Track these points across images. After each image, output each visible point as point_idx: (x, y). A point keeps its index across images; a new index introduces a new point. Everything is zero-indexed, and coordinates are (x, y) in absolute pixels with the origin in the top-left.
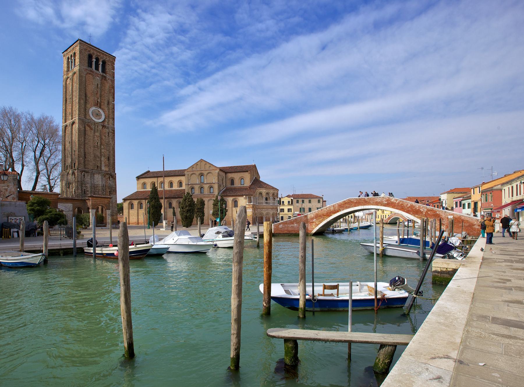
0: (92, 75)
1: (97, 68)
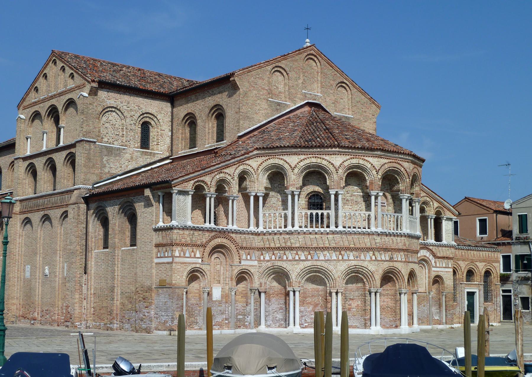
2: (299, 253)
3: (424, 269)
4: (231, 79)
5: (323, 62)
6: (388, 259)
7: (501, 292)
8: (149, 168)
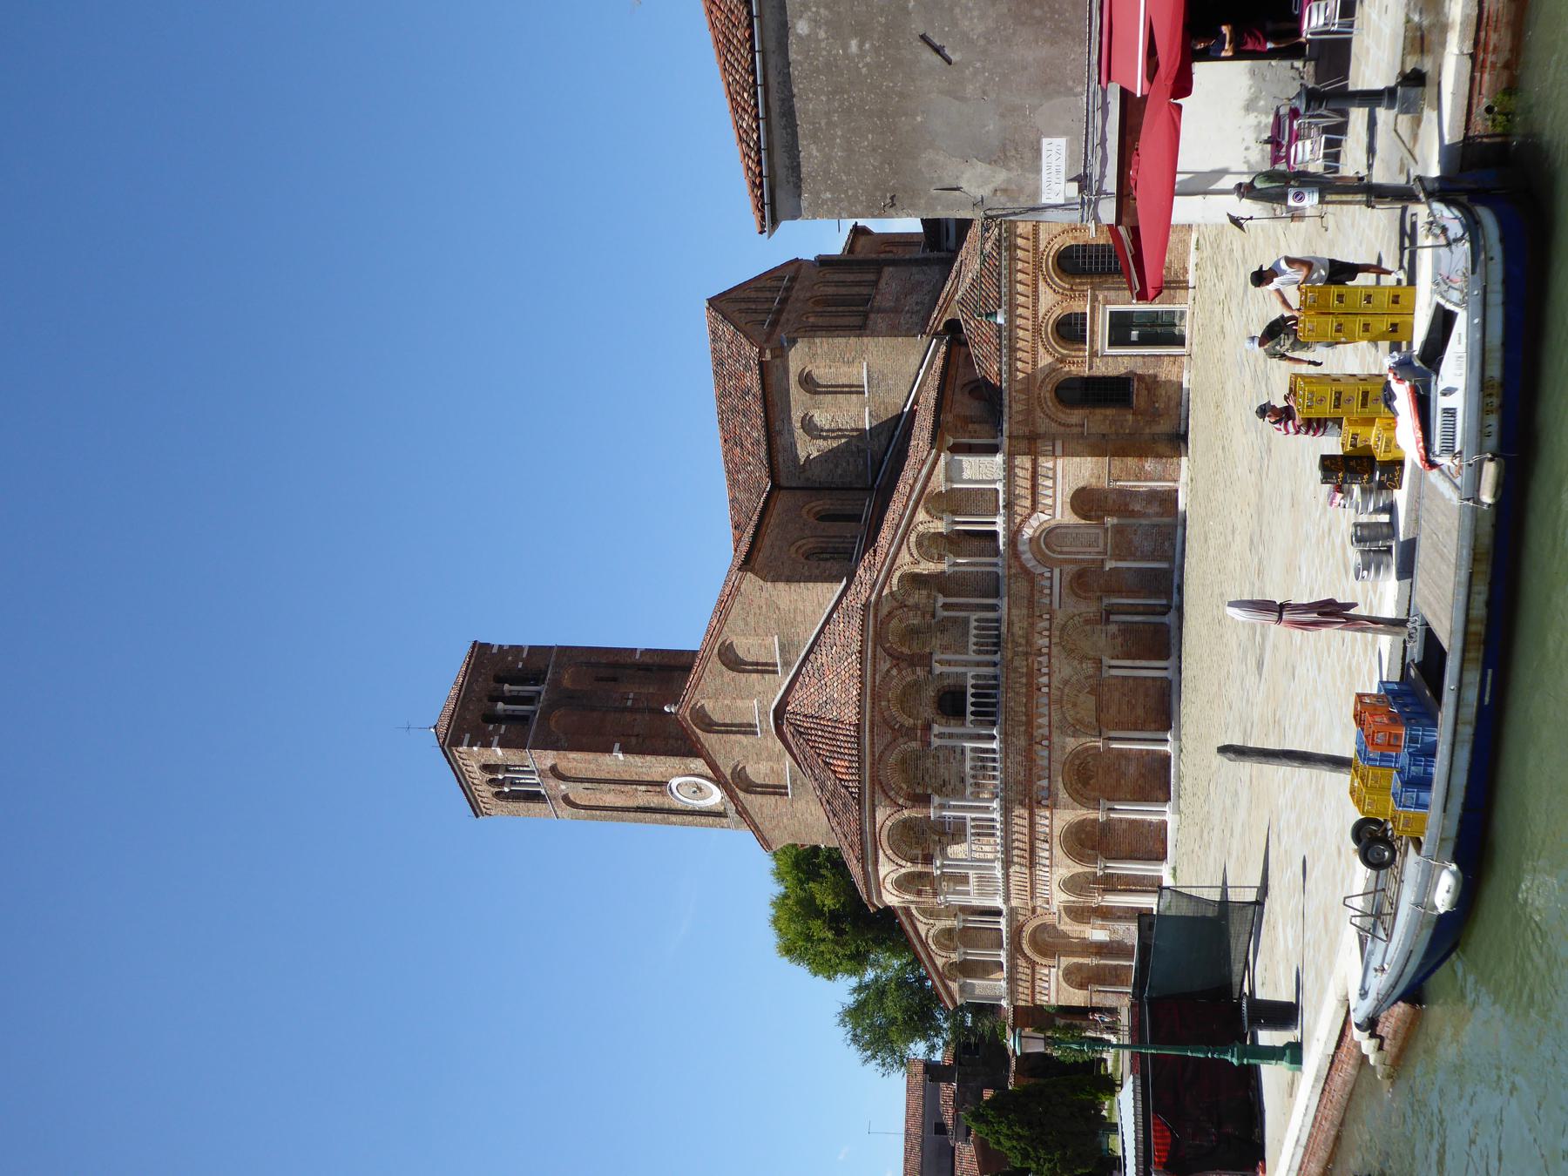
3: (1058, 530)
5: (697, 696)
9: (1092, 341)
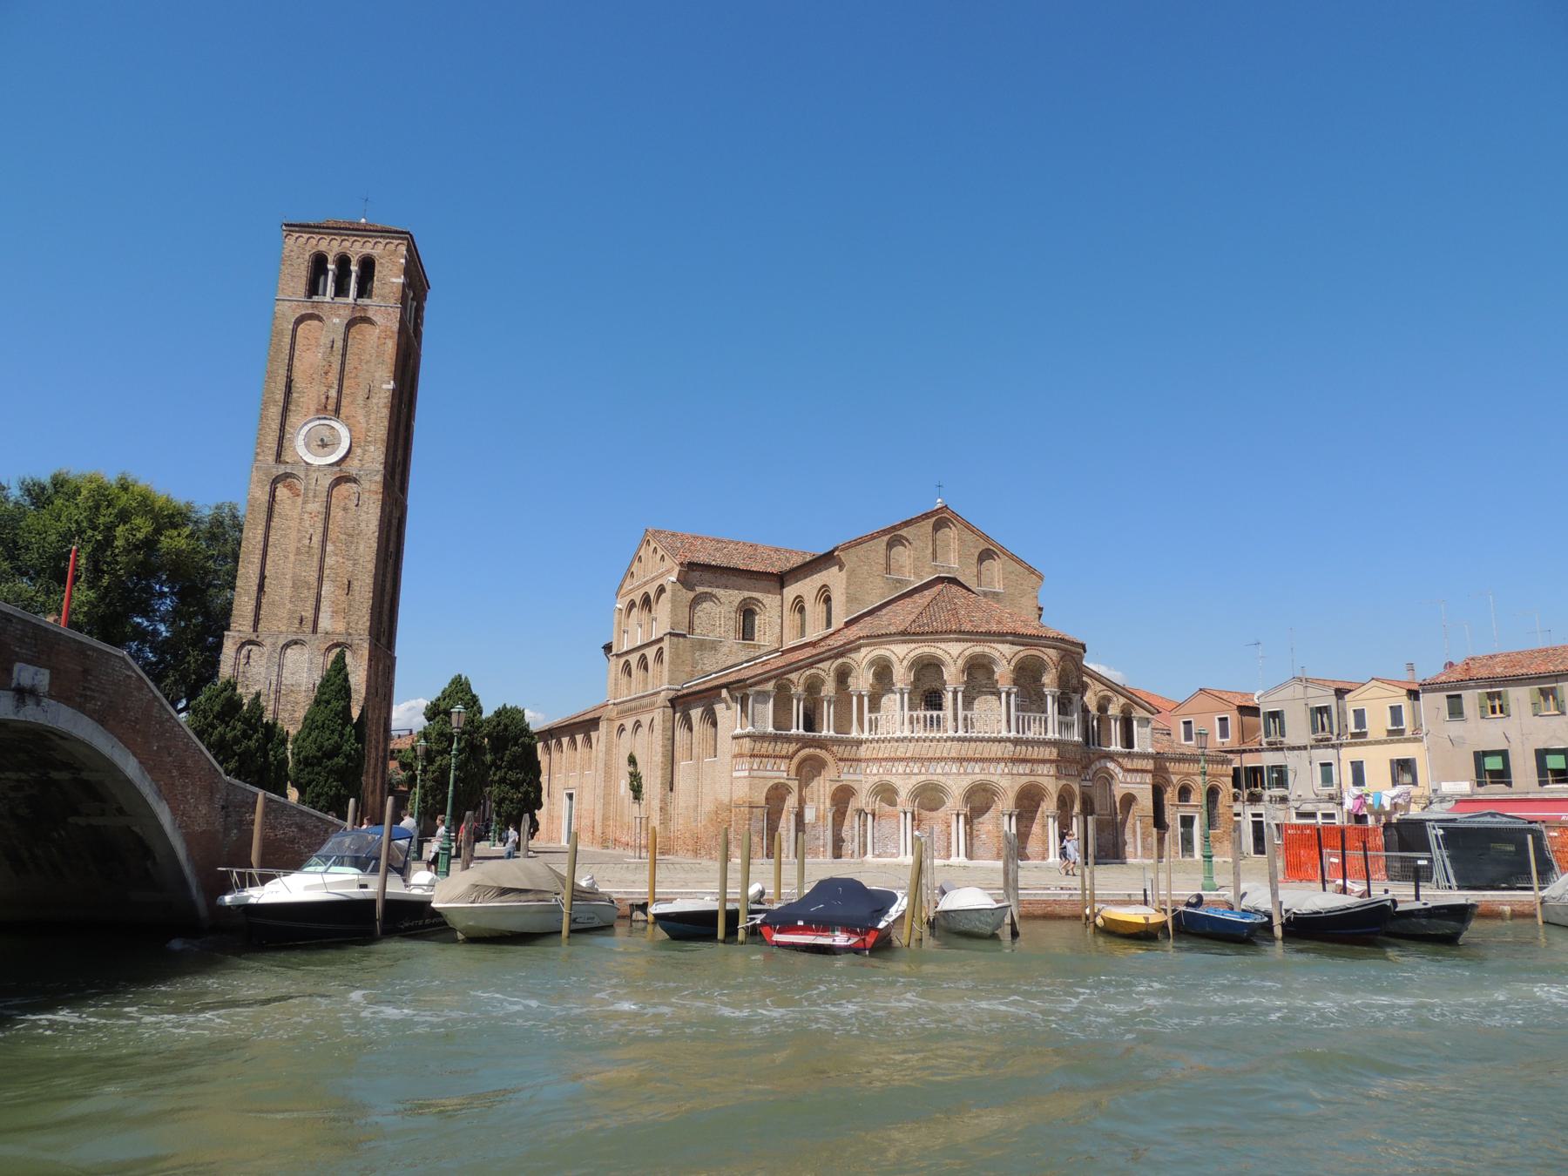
0: (319, 318)
1: (341, 290)
2: (911, 764)
4: (836, 554)
5: (959, 525)
6: (1027, 771)
7: (1250, 816)
8: (752, 663)
9: (1183, 806)
